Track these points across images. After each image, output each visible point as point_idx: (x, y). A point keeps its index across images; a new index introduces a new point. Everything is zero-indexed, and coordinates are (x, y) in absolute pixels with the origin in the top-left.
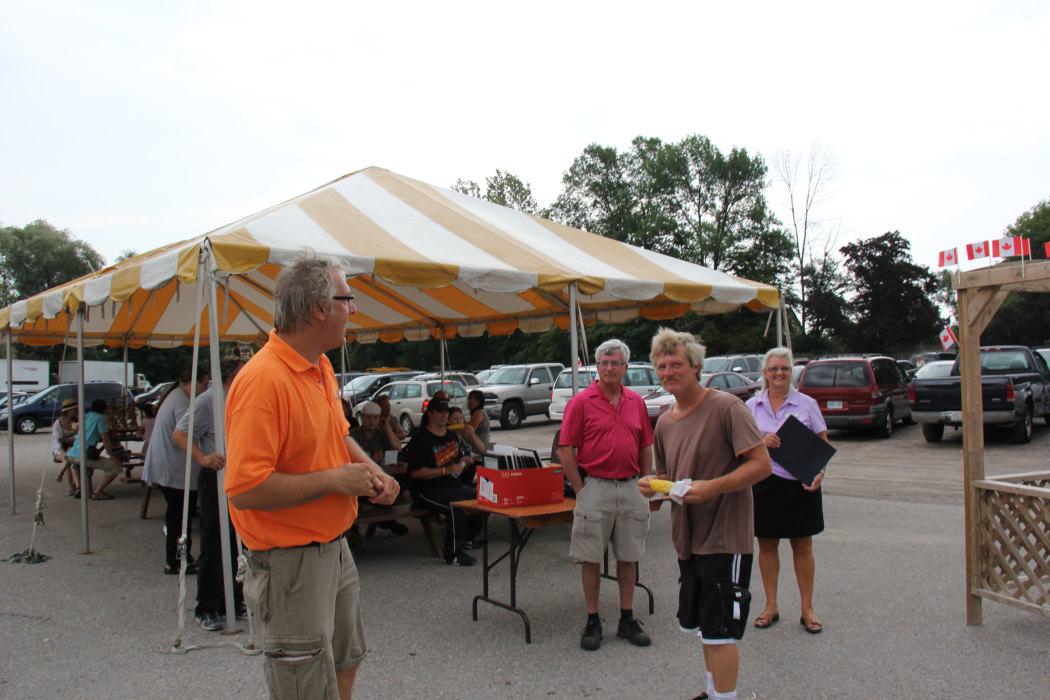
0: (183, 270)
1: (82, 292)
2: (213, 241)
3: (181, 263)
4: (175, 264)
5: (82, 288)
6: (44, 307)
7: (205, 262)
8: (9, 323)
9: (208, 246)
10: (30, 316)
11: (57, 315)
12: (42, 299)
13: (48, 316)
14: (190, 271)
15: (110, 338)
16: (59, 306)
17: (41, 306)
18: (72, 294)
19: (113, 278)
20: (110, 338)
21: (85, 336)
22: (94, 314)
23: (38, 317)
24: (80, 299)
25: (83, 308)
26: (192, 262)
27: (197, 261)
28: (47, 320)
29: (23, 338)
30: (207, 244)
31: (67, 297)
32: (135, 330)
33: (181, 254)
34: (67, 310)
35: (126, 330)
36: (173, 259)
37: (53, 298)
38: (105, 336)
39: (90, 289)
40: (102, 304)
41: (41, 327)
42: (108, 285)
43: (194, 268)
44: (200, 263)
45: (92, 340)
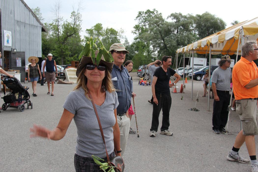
0: (236, 35)
1: (211, 40)
2: (244, 27)
3: (235, 33)
4: (234, 33)
5: (211, 39)
6: (202, 44)
7: (241, 33)
8: (193, 48)
9: (242, 29)
10: (198, 46)
11: (205, 46)
12: (201, 42)
13: (202, 46)
14: (237, 35)
15: (223, 52)
16: (205, 44)
17: (201, 43)
18: (209, 41)
19: (219, 37)
20: (223, 52)
21: (212, 51)
22: (214, 46)
23: (200, 47)
24: (210, 42)
25: (211, 45)
26: (238, 33)
27: (239, 33)
28: (203, 48)
29: (198, 52)
30: (242, 28)
31: (207, 41)
32: (231, 49)
33: (235, 31)
34: (207, 45)
35: (228, 49)
36: (233, 32)
37: (205, 41)
38: (222, 51)
39: (213, 38)
40: (216, 43)
41: (201, 49)
42: (217, 38)
43: (238, 35)
44: (239, 33)
45: (217, 52)
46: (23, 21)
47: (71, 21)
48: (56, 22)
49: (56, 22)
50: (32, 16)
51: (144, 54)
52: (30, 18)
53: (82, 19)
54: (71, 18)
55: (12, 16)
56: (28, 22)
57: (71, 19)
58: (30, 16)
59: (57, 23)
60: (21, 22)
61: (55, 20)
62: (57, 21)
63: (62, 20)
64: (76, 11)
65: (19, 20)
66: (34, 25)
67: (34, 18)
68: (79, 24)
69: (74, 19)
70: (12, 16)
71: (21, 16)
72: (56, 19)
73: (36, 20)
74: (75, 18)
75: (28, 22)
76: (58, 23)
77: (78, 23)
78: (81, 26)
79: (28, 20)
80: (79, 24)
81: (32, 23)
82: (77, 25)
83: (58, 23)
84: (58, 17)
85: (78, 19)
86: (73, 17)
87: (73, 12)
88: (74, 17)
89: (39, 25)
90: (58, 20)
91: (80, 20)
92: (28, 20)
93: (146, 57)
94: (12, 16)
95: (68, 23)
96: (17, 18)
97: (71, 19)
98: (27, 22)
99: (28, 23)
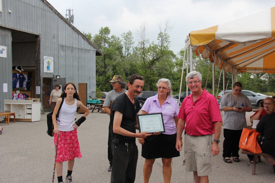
46: (69, 45)
47: (157, 42)
48: (142, 44)
49: (142, 44)
50: (82, 40)
51: (252, 77)
52: (80, 41)
53: (170, 39)
54: (158, 39)
55: (55, 40)
56: (76, 46)
57: (159, 41)
58: (80, 40)
59: (143, 45)
60: (66, 47)
61: (141, 43)
62: (143, 43)
63: (148, 42)
64: (163, 32)
65: (64, 44)
66: (73, 46)
67: (86, 42)
68: (167, 46)
69: (161, 40)
70: (54, 41)
71: (67, 40)
72: (141, 42)
73: (87, 43)
74: (163, 39)
75: (76, 46)
76: (144, 46)
77: (165, 44)
78: (169, 48)
79: (76, 44)
80: (167, 46)
81: (83, 47)
82: (164, 47)
83: (144, 46)
84: (143, 40)
85: (166, 40)
86: (160, 39)
87: (160, 33)
88: (161, 38)
89: (92, 48)
90: (144, 43)
91: (168, 41)
92: (76, 44)
93: (252, 80)
94: (55, 41)
95: (155, 45)
96: (62, 42)
97: (159, 41)
98: (76, 46)
99: (76, 47)
